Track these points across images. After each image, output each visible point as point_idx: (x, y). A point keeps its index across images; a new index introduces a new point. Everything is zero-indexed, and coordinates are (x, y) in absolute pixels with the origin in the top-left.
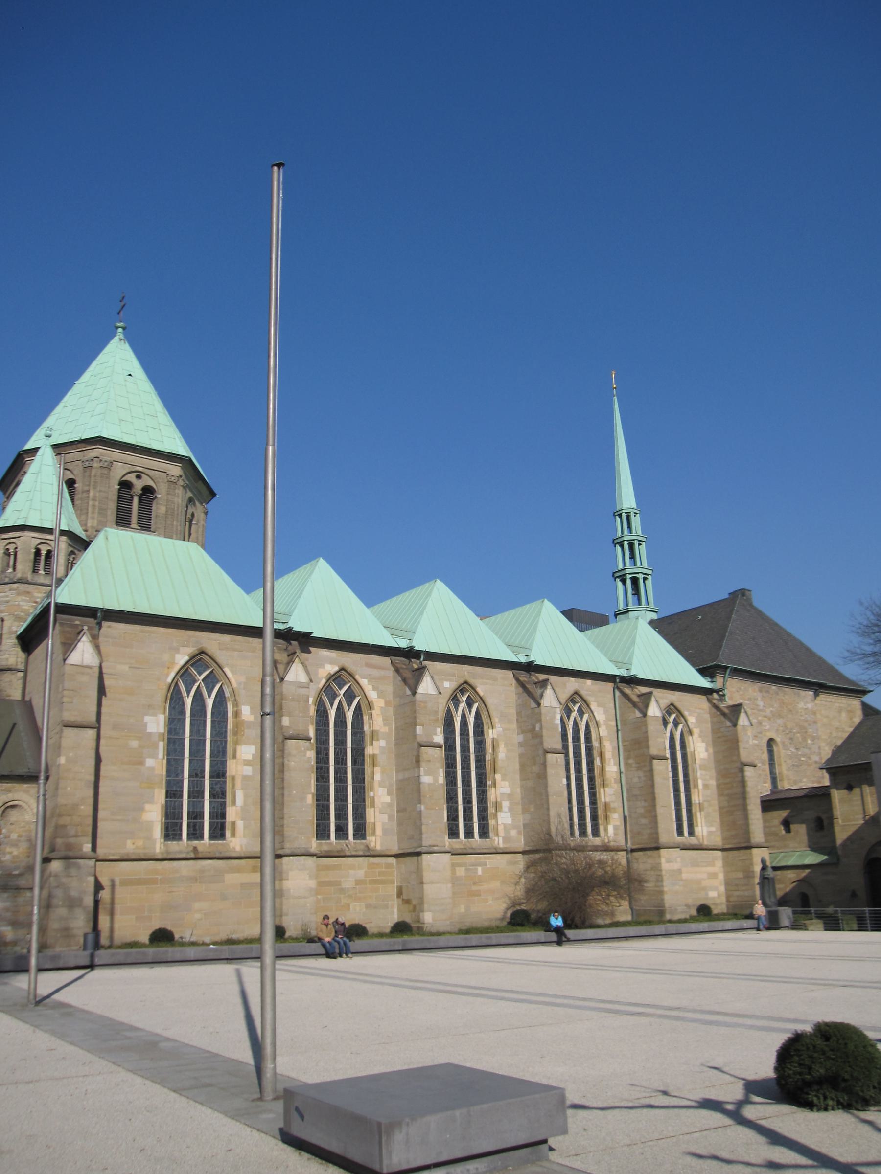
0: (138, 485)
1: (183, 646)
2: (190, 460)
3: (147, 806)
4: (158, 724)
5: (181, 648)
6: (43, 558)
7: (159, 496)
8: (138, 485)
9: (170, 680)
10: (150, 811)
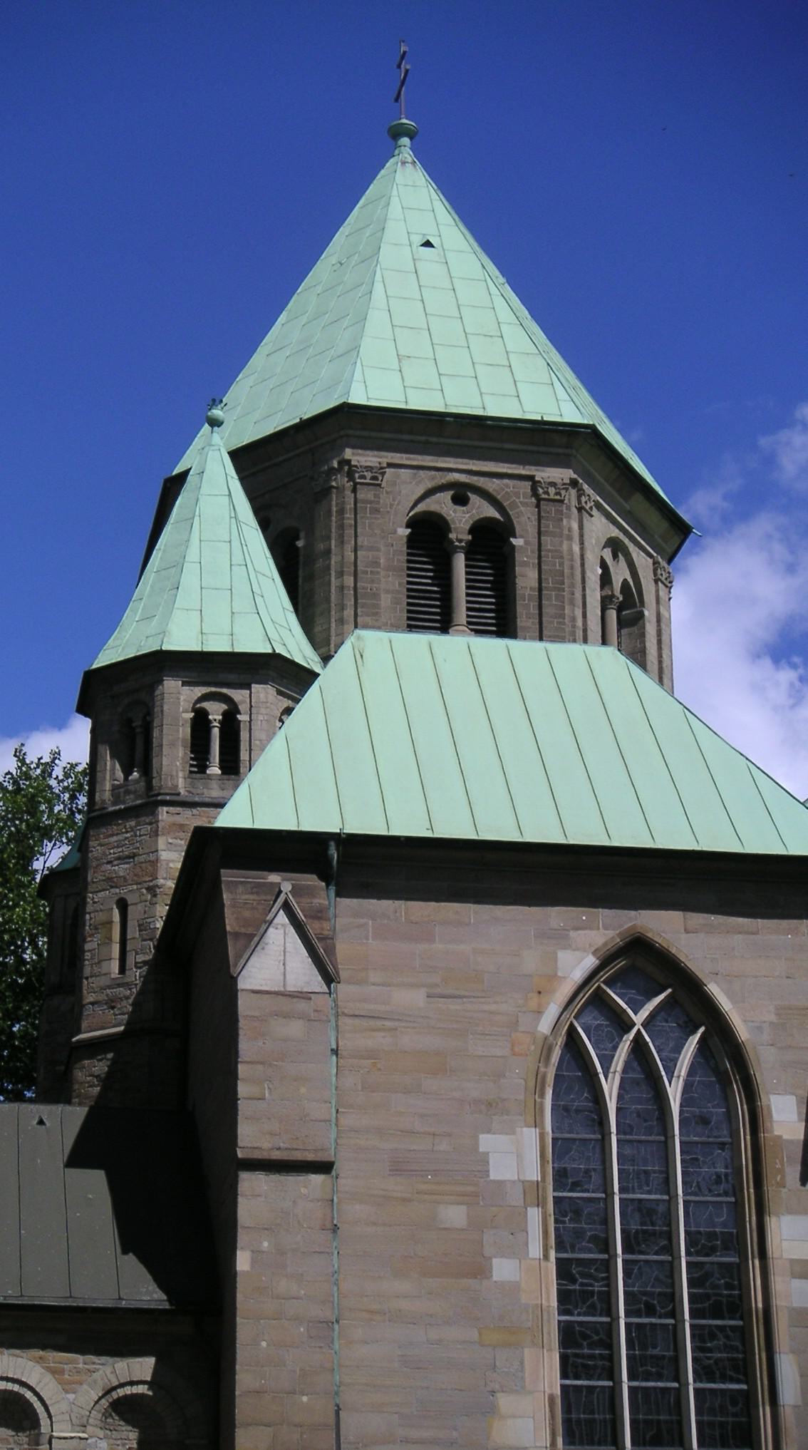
0: (461, 520)
1: (576, 929)
2: (593, 428)
3: (504, 1402)
4: (520, 1157)
5: (572, 934)
6: (216, 732)
7: (517, 542)
8: (461, 520)
9: (545, 1026)
10: (514, 1417)
